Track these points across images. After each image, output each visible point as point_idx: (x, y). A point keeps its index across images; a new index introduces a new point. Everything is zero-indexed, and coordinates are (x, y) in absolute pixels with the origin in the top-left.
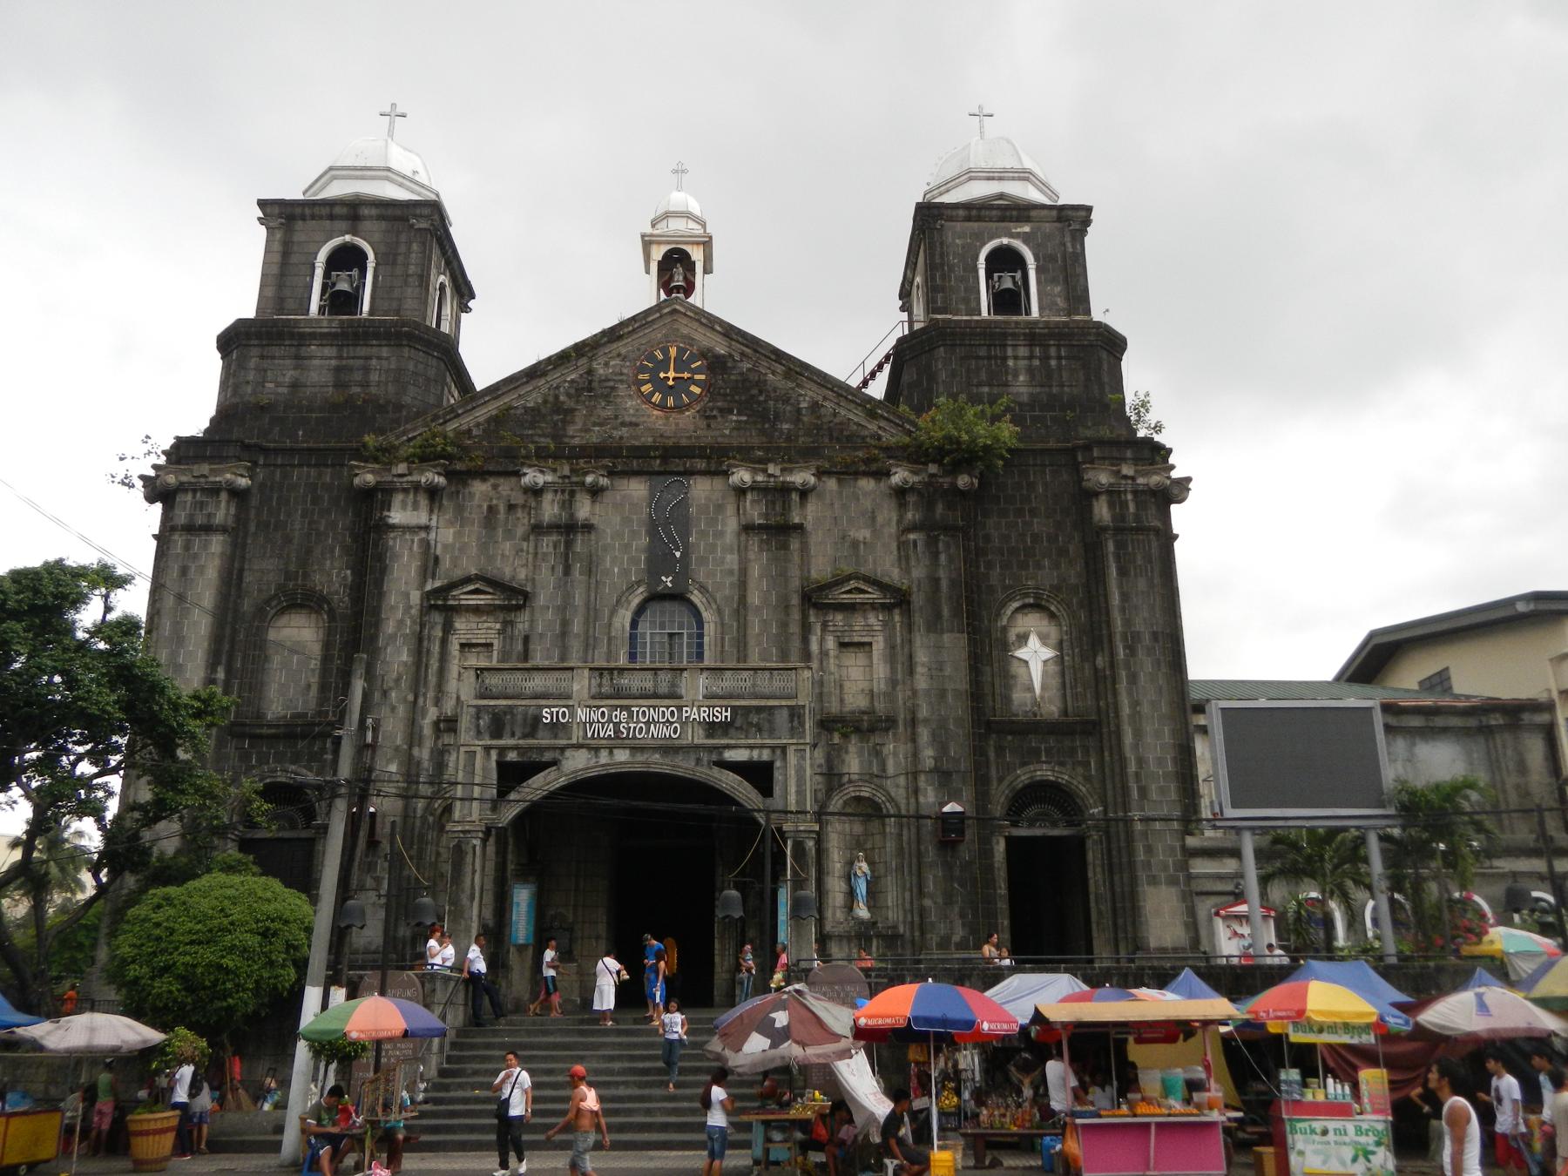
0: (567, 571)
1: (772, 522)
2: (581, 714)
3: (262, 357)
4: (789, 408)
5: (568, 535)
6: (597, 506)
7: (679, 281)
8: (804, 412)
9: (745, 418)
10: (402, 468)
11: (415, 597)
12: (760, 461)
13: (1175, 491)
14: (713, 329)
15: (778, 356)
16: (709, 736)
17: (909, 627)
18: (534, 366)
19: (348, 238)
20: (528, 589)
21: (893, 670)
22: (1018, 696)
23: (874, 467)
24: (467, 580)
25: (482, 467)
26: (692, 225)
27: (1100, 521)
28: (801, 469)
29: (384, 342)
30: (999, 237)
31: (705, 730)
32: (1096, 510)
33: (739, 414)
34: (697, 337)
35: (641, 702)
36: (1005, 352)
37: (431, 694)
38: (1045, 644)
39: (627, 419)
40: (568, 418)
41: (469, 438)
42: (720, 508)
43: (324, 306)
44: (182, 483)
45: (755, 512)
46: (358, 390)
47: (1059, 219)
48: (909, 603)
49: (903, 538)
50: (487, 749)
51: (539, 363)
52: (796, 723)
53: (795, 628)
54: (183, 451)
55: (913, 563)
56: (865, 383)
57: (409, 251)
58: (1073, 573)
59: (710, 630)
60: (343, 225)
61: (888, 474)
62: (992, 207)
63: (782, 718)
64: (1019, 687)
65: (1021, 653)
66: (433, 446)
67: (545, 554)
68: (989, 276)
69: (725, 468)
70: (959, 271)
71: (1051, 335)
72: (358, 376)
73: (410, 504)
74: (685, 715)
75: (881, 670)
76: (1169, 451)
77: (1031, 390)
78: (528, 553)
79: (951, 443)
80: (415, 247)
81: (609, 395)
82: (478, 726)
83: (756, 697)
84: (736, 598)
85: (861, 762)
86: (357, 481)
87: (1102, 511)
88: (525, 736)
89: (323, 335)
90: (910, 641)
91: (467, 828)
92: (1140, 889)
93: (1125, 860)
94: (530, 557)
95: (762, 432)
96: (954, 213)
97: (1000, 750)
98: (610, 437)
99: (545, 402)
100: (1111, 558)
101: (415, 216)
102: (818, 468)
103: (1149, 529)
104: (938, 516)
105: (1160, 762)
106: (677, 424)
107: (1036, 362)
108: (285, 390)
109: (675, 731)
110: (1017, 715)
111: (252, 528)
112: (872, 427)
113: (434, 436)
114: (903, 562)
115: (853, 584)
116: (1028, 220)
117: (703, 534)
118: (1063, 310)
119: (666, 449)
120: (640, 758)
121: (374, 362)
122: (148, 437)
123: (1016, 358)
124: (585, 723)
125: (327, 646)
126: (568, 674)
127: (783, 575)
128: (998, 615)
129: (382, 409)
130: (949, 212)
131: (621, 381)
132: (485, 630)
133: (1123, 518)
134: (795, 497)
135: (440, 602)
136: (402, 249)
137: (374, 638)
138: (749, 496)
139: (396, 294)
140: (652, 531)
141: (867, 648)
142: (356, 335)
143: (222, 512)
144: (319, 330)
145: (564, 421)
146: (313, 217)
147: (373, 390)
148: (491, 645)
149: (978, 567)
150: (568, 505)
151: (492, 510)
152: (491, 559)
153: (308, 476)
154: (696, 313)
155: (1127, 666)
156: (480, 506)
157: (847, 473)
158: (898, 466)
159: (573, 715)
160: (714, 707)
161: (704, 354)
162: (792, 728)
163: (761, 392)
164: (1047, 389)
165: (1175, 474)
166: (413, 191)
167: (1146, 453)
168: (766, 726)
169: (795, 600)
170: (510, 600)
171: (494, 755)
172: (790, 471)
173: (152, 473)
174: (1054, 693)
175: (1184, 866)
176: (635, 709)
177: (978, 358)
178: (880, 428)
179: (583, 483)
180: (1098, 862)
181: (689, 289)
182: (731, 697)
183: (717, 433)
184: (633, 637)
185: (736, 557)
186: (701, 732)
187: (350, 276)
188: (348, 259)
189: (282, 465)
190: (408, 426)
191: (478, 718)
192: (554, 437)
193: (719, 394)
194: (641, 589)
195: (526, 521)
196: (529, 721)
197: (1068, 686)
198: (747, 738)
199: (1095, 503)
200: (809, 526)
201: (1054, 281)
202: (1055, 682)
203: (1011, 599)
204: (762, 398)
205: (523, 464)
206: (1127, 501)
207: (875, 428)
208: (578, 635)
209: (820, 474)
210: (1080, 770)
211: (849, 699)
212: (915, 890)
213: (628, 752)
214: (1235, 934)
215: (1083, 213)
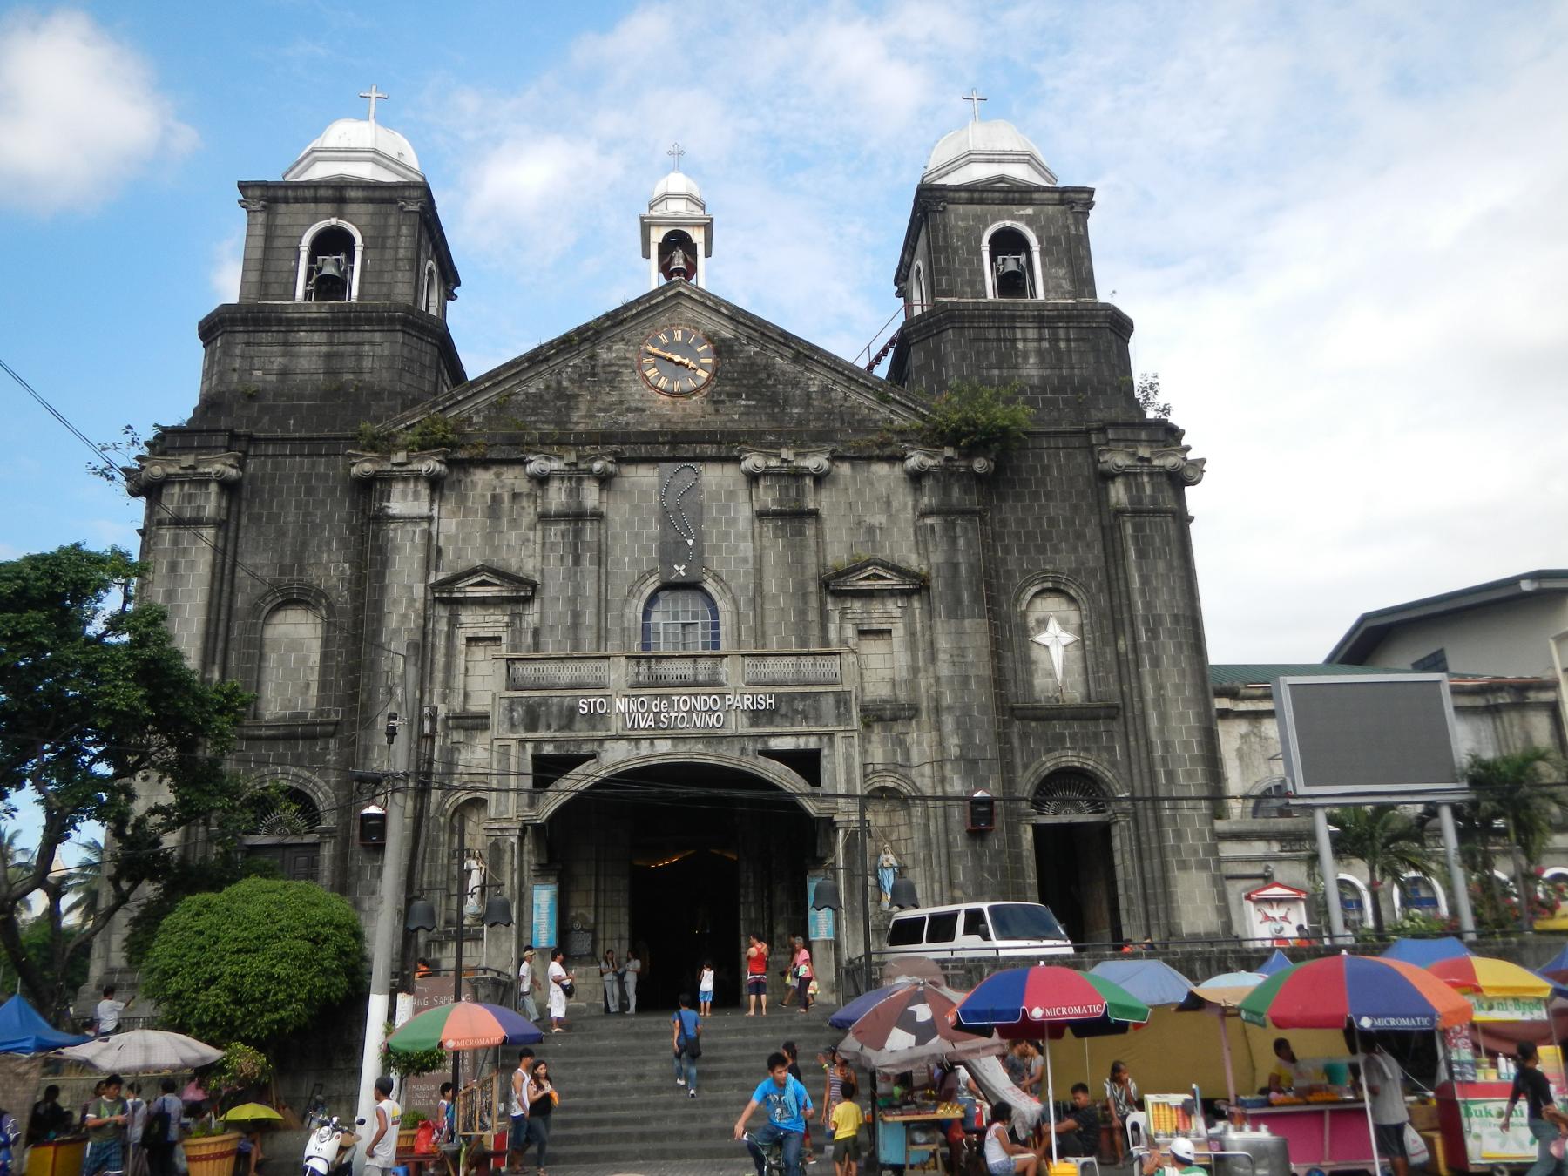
0: (577, 561)
1: (786, 508)
2: (620, 704)
3: (248, 344)
4: (798, 392)
5: (576, 524)
6: (605, 495)
7: (679, 262)
8: (814, 396)
9: (753, 403)
10: (401, 457)
11: (419, 590)
12: (772, 446)
13: (1190, 473)
14: (719, 312)
15: (786, 339)
16: (754, 724)
17: (931, 614)
18: (536, 350)
19: (333, 221)
20: (537, 579)
21: (914, 658)
22: (1039, 682)
23: (888, 451)
24: (474, 572)
25: (484, 454)
26: (692, 207)
27: (1117, 503)
28: (815, 453)
29: (376, 328)
30: (1002, 219)
31: (749, 718)
32: (1113, 493)
33: (748, 398)
34: (702, 320)
35: (681, 690)
36: (1014, 334)
37: (437, 690)
38: (1065, 629)
39: (633, 404)
40: (572, 404)
41: (469, 426)
42: (731, 494)
43: (310, 292)
44: (169, 475)
45: (767, 496)
46: (351, 377)
47: (1061, 202)
48: (928, 589)
49: (920, 523)
50: (523, 742)
51: (541, 347)
52: (842, 710)
53: (813, 616)
54: (167, 441)
55: (931, 548)
56: (870, 367)
57: (399, 235)
58: (1093, 556)
59: (726, 619)
60: (325, 208)
61: (903, 459)
62: (994, 190)
63: (828, 704)
64: (1040, 673)
65: (1042, 638)
66: (433, 433)
67: (553, 544)
68: (993, 259)
69: (736, 453)
70: (963, 253)
71: (1060, 318)
72: (350, 362)
73: (410, 495)
74: (727, 703)
75: (903, 658)
76: (1183, 432)
77: (1041, 372)
78: (535, 543)
79: (968, 425)
80: (404, 230)
81: (613, 380)
83: (800, 683)
84: (751, 586)
86: (354, 470)
87: (1118, 493)
88: (561, 729)
89: (313, 321)
90: (931, 627)
91: (504, 825)
92: (1171, 874)
93: (1154, 845)
94: (538, 547)
95: (772, 417)
96: (957, 195)
97: (1024, 736)
98: (616, 423)
99: (548, 387)
100: (1130, 542)
101: (404, 199)
102: (832, 452)
103: (1166, 512)
104: (954, 500)
105: (1186, 745)
106: (684, 409)
107: (1046, 345)
108: (273, 378)
109: (718, 721)
110: (1037, 701)
111: (244, 521)
112: (884, 412)
113: (435, 423)
114: (921, 546)
115: (871, 570)
116: (1030, 202)
117: (715, 521)
118: (1069, 292)
119: (674, 434)
120: (682, 748)
121: (367, 348)
122: (129, 427)
123: (1025, 340)
125: (326, 642)
126: (605, 663)
127: (799, 561)
128: (1017, 600)
129: (377, 395)
130: (951, 194)
131: (626, 366)
132: (491, 622)
133: (1140, 501)
134: (809, 482)
135: (445, 595)
136: (392, 232)
137: (377, 633)
138: (762, 483)
139: (387, 278)
140: (665, 516)
141: (886, 636)
142: (347, 321)
143: (211, 503)
144: (308, 315)
145: (568, 407)
146: (297, 200)
147: (367, 377)
148: (499, 638)
149: (995, 552)
150: (575, 493)
151: (496, 499)
152: (496, 549)
154: (701, 296)
155: (1150, 649)
156: (483, 496)
157: (861, 458)
158: (913, 449)
159: (610, 705)
160: (757, 694)
161: (709, 338)
162: (839, 716)
163: (769, 376)
164: (1057, 372)
165: (1190, 456)
166: (398, 174)
167: (1160, 435)
168: (812, 713)
169: (813, 587)
170: (518, 591)
171: (529, 747)
172: (804, 455)
173: (135, 465)
174: (1077, 678)
175: (1214, 851)
177: (987, 340)
178: (892, 411)
179: (591, 471)
180: (1127, 848)
181: (690, 270)
182: (774, 683)
183: (726, 418)
184: (646, 629)
185: (750, 544)
186: (745, 720)
187: (338, 260)
188: (332, 242)
190: (407, 413)
191: (512, 710)
192: (557, 423)
193: (727, 378)
194: (653, 579)
195: (532, 511)
196: (565, 712)
197: (1090, 670)
198: (792, 725)
199: (1111, 486)
200: (824, 513)
201: (1058, 263)
202: (1077, 667)
203: (1031, 584)
204: (770, 382)
205: (529, 451)
206: (1143, 483)
207: (887, 412)
208: (590, 627)
209: (835, 458)
210: (1105, 755)
211: (869, 688)
212: (945, 883)
213: (669, 742)
214: (1267, 918)
215: (1085, 196)
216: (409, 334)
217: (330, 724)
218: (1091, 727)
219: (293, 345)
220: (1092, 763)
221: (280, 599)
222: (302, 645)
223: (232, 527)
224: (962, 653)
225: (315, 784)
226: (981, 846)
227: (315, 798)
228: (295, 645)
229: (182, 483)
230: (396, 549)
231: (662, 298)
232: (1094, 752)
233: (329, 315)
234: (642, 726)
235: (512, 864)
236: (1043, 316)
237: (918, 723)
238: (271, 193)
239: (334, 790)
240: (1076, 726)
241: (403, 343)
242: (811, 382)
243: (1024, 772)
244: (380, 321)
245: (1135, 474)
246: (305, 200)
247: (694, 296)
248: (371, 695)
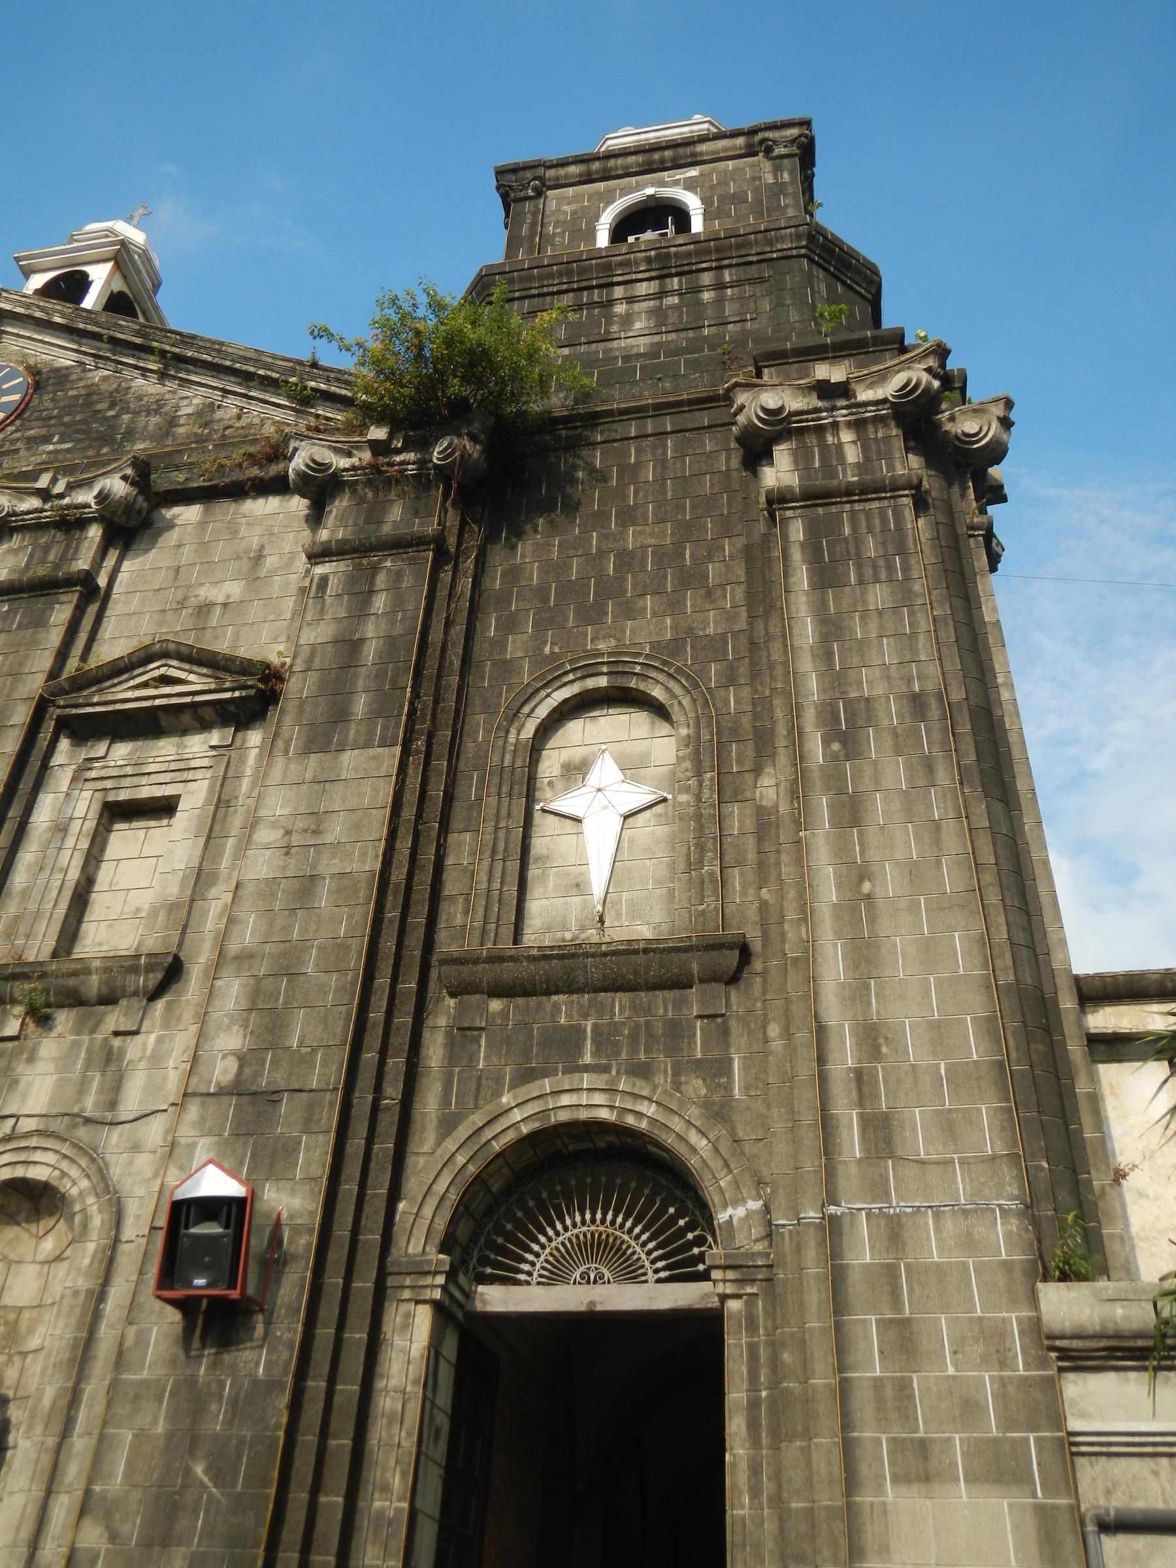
4: (155, 420)
9: (69, 445)
33: (60, 442)
47: (750, 152)
85: (60, 1084)
100: (797, 555)
103: (895, 487)
163: (112, 405)
193: (37, 419)
203: (552, 682)
206: (839, 446)
210: (696, 1086)
215: (794, 132)
218: (662, 1004)
220: (650, 1110)
224: (317, 820)
226: (213, 1366)
232: (663, 1080)
236: (668, 255)
237: (169, 1007)
240: (619, 1003)
242: (185, 402)
243: (439, 1142)
245: (820, 430)
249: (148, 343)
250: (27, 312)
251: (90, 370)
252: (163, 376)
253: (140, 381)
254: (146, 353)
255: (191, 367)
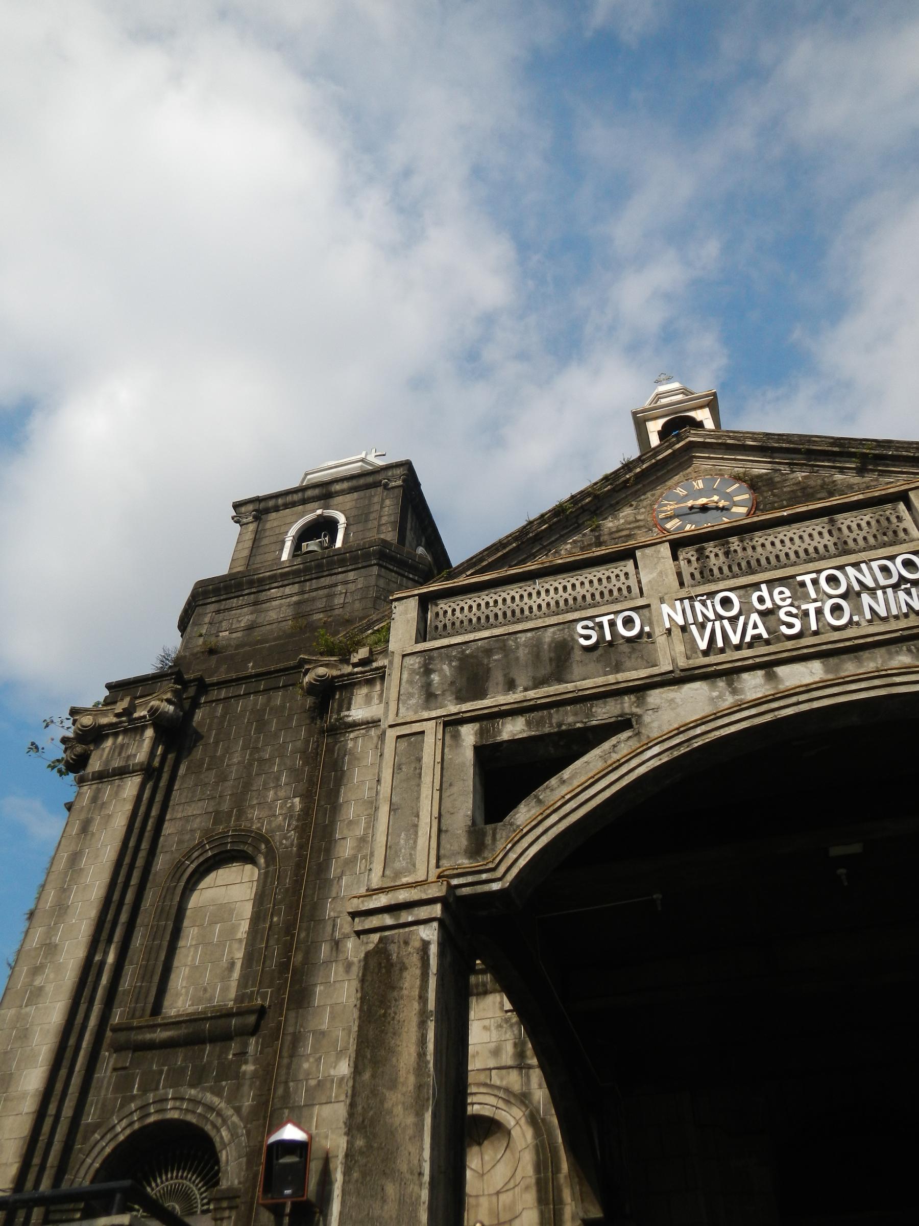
3: (218, 612)
18: (524, 527)
19: (319, 512)
51: (530, 523)
82: (428, 685)
88: (538, 683)
111: (182, 770)
120: (850, 668)
121: (339, 588)
124: (684, 629)
131: (639, 527)
136: (377, 507)
137: (322, 868)
142: (319, 567)
146: (286, 506)
147: (336, 612)
153: (255, 704)
171: (469, 734)
176: (807, 579)
189: (224, 699)
191: (427, 671)
196: (546, 655)
216: (386, 568)
217: (249, 1012)
219: (264, 602)
221: (210, 853)
222: (231, 912)
223: (165, 777)
225: (219, 1114)
227: (217, 1140)
228: (224, 912)
229: (116, 735)
230: (355, 758)
231: (670, 451)
233: (301, 566)
234: (735, 639)
235: (423, 998)
238: (262, 505)
239: (247, 1120)
241: (379, 576)
244: (355, 559)
246: (294, 504)
247: (708, 440)
248: (310, 949)
249: (846, 450)
250: (720, 441)
251: (788, 474)
252: (861, 471)
253: (838, 477)
254: (842, 456)
255: (888, 462)
